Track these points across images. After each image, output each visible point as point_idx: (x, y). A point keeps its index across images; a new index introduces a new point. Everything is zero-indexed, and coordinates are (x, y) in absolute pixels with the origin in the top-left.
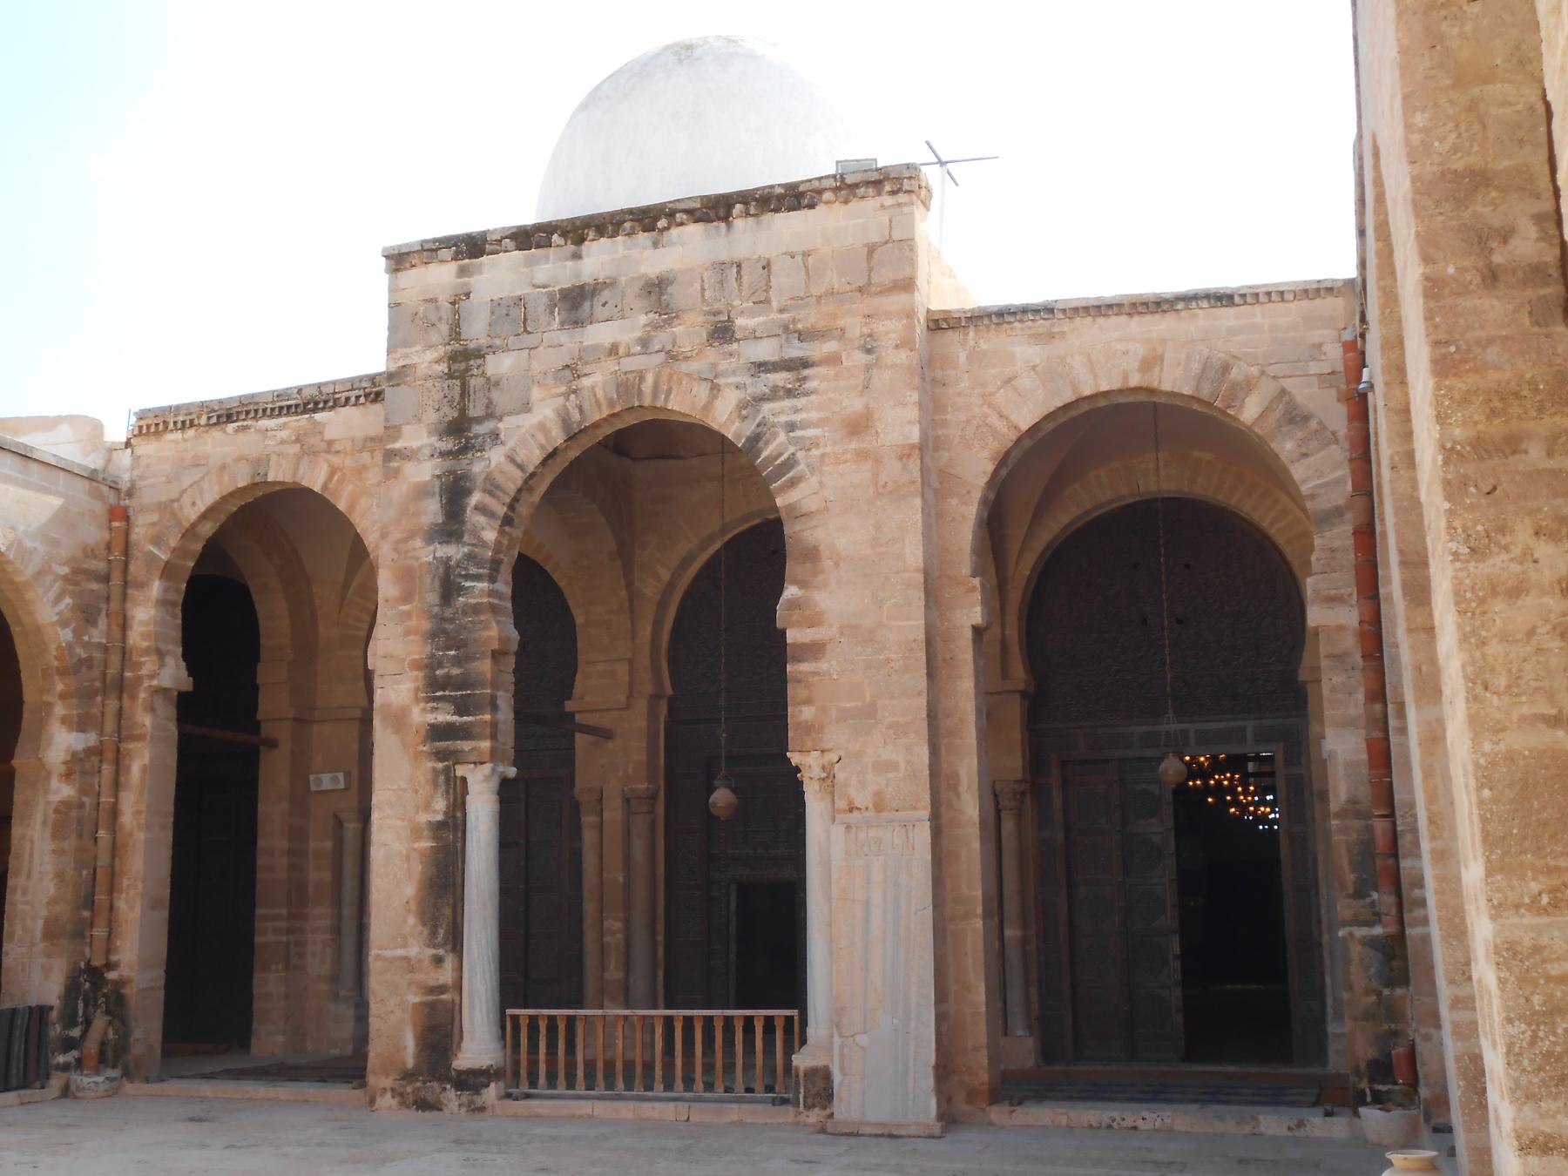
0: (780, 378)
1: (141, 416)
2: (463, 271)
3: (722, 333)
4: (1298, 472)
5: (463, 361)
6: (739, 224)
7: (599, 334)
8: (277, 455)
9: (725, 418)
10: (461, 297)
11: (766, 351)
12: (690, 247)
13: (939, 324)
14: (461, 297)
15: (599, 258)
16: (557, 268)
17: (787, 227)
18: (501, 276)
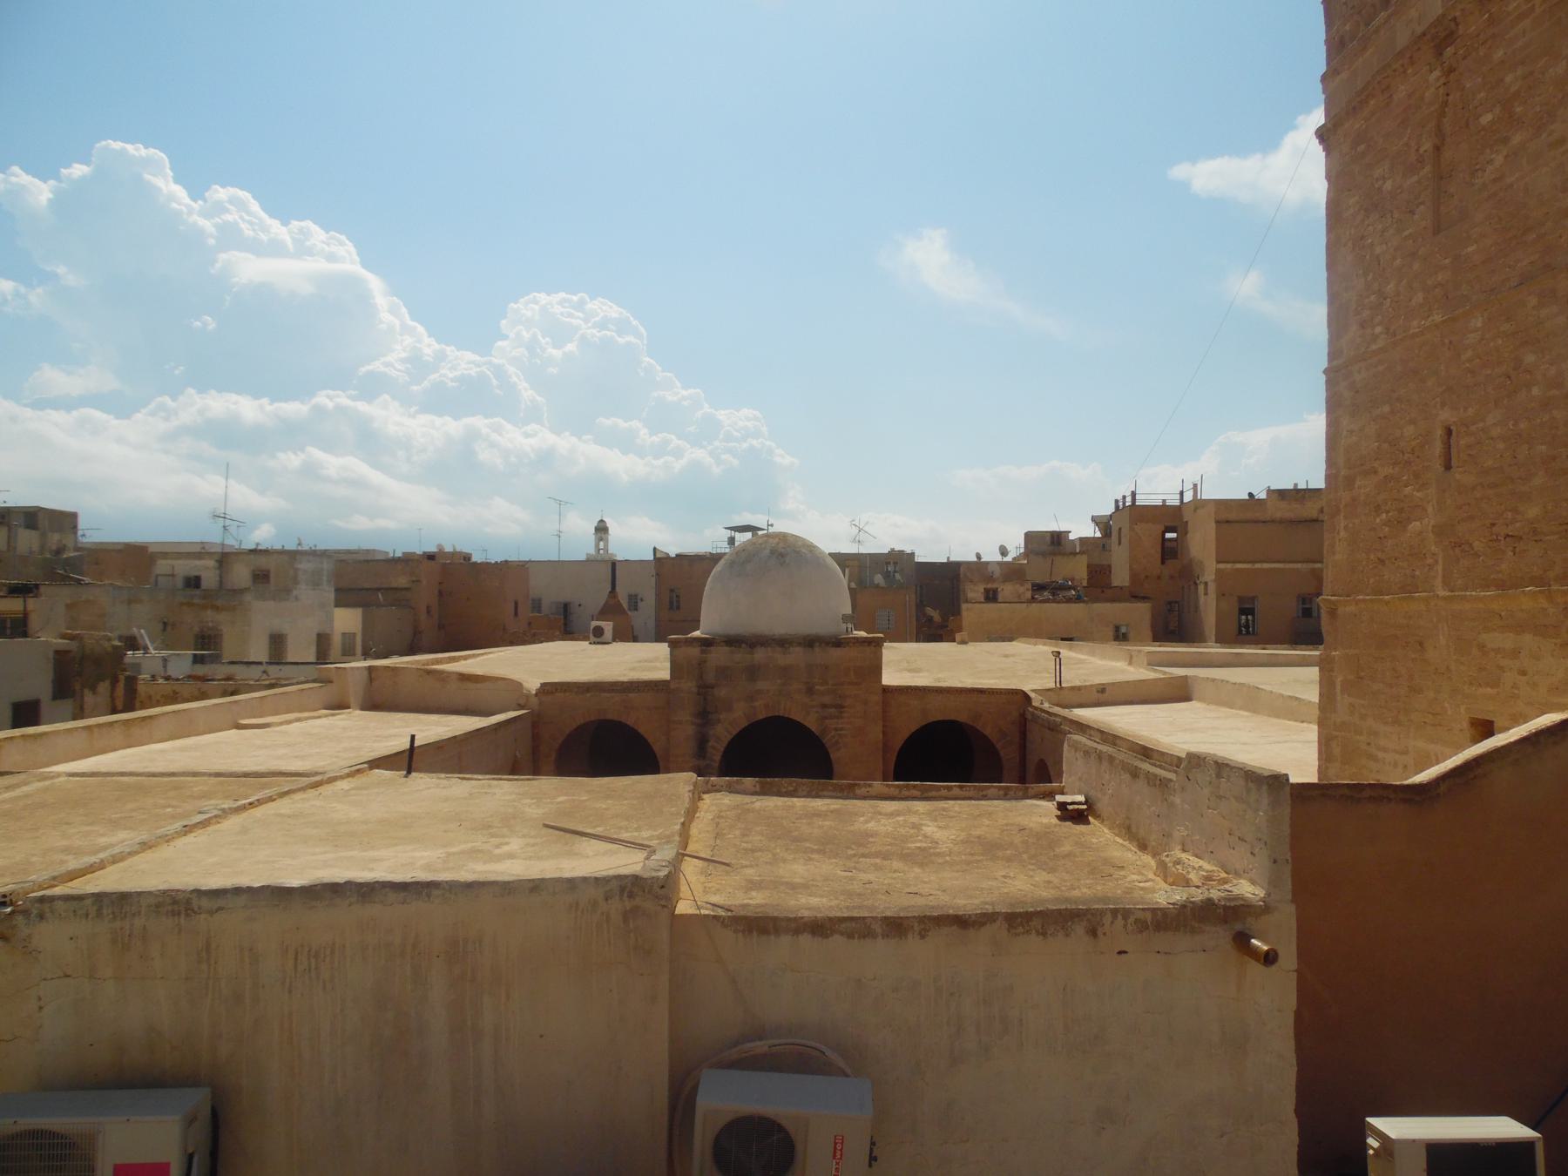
0: (832, 710)
1: (544, 685)
2: (703, 652)
3: (810, 691)
4: (1002, 753)
5: (704, 689)
6: (817, 649)
7: (761, 685)
8: (612, 710)
10: (701, 664)
11: (827, 700)
12: (796, 656)
13: (888, 690)
14: (701, 664)
15: (760, 655)
17: (836, 654)
18: (719, 656)
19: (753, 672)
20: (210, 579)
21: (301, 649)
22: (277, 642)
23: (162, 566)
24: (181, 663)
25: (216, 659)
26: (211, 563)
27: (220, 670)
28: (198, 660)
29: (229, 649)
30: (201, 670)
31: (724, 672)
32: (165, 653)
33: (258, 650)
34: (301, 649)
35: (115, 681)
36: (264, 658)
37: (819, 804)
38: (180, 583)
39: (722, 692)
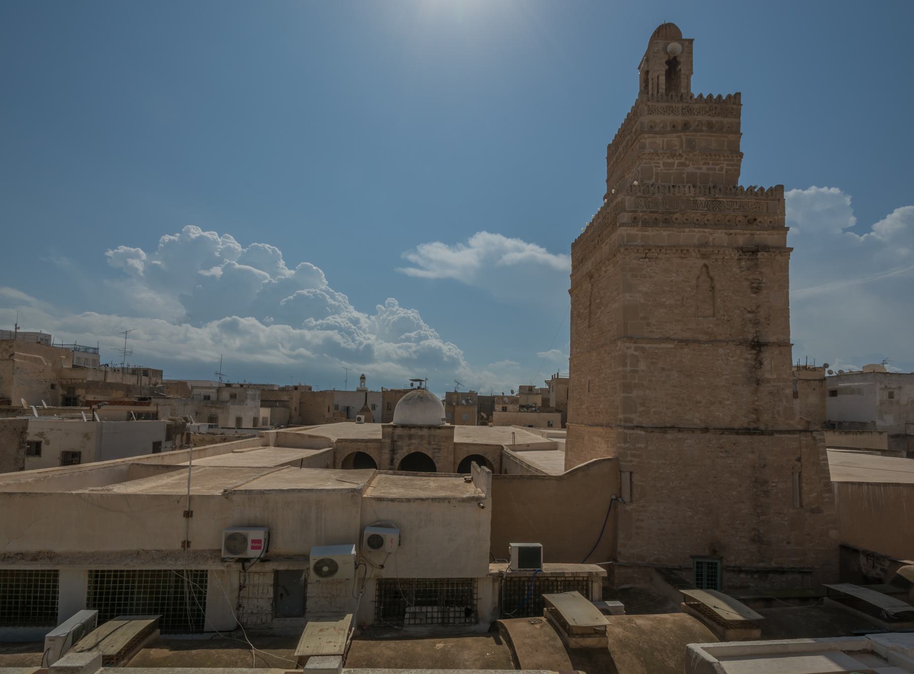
7: (413, 441)
9: (430, 454)
15: (413, 431)
16: (406, 432)
19: (410, 437)
20: (213, 397)
21: (247, 423)
22: (239, 420)
23: (196, 391)
24: (204, 427)
25: (216, 426)
26: (214, 391)
27: (219, 431)
28: (210, 427)
29: (221, 423)
30: (211, 430)
31: (400, 436)
32: (199, 424)
33: (232, 423)
34: (247, 423)
35: (183, 434)
36: (234, 426)
37: (407, 477)
38: (202, 398)
39: (399, 443)
